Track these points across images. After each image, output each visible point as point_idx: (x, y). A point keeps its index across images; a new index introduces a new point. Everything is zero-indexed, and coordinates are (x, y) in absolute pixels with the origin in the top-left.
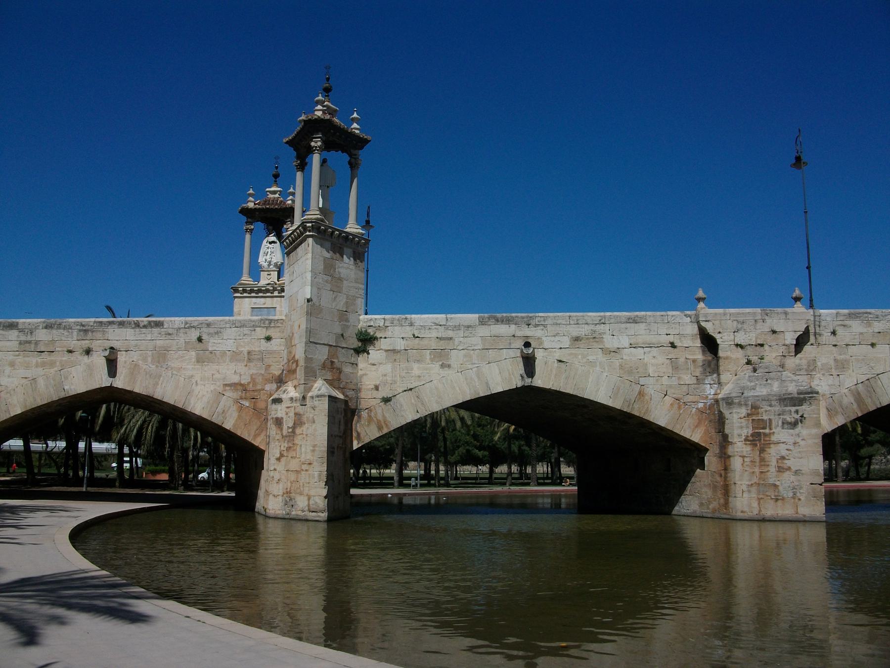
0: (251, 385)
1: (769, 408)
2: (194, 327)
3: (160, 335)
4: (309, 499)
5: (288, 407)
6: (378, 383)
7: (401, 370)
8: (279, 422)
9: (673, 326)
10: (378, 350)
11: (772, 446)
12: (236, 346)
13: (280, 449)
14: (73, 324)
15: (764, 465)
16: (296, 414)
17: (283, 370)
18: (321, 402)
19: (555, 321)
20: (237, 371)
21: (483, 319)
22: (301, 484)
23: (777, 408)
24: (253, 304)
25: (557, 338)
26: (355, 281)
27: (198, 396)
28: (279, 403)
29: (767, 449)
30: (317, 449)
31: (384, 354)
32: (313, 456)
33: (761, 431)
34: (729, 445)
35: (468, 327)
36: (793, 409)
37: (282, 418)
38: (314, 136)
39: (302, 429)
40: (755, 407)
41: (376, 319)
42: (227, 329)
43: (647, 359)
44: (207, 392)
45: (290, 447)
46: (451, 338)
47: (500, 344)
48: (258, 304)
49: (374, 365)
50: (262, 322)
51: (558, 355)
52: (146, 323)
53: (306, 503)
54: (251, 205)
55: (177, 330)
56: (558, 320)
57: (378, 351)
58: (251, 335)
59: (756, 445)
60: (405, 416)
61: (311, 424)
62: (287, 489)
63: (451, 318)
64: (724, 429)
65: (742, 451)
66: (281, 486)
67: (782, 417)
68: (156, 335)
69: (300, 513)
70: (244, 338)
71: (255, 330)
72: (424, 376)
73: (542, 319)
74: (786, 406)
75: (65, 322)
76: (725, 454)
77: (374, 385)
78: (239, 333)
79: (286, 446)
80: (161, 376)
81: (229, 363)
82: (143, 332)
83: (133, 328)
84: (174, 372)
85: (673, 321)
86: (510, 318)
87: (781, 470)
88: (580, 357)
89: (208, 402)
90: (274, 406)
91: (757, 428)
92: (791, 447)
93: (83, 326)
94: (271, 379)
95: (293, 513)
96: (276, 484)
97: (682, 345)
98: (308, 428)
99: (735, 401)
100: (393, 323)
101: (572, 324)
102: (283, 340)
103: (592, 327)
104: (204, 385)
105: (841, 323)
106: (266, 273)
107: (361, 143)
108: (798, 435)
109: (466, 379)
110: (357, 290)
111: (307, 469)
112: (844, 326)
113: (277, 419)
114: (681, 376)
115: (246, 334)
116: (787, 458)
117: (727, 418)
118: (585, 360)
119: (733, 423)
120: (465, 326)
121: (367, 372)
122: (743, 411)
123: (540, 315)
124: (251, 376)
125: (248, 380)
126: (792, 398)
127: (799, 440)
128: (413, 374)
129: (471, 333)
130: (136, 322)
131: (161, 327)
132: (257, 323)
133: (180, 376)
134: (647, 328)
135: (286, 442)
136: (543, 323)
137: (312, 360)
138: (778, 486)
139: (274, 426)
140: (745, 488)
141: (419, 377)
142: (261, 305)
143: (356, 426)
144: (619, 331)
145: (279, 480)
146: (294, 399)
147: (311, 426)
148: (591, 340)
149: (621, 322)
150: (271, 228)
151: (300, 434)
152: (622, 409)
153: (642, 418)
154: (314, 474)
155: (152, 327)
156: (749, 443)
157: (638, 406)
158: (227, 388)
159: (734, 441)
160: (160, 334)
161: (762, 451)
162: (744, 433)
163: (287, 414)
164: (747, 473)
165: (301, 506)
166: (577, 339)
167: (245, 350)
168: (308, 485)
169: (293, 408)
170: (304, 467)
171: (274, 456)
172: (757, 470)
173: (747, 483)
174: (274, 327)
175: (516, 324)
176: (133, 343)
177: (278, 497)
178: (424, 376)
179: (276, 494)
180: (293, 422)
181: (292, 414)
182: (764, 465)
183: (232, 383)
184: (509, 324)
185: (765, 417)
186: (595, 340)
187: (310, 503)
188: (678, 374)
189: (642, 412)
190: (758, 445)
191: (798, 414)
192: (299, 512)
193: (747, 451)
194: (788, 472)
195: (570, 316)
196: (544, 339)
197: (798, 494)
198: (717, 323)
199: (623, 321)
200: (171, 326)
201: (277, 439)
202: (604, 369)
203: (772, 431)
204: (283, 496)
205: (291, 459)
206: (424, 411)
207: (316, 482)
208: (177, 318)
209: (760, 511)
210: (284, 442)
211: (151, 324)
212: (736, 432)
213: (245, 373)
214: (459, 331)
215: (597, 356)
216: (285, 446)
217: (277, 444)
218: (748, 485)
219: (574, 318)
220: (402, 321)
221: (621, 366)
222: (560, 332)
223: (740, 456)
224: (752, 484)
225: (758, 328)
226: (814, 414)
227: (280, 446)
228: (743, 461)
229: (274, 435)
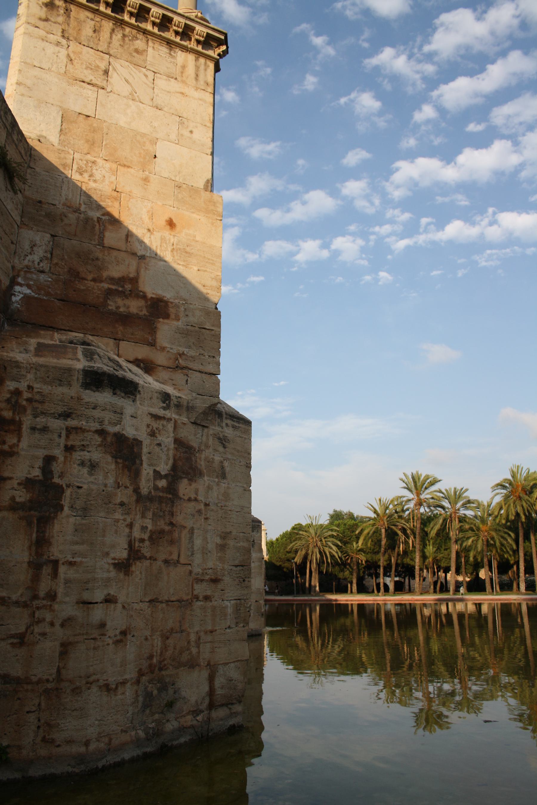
13: (130, 535)
16: (178, 442)
18: (238, 433)
22: (193, 637)
28: (126, 393)
30: (231, 543)
32: (221, 559)
39: (194, 485)
45: (162, 532)
61: (217, 480)
62: (151, 657)
79: (150, 527)
96: (112, 647)
111: (209, 593)
135: (150, 514)
145: (124, 633)
146: (174, 401)
147: (218, 484)
151: (190, 500)
163: (152, 434)
165: (193, 699)
168: (209, 638)
170: (200, 589)
177: (120, 690)
179: (112, 680)
180: (171, 462)
201: (118, 501)
204: (138, 682)
210: (143, 516)
216: (144, 528)
217: (117, 516)
227: (131, 526)
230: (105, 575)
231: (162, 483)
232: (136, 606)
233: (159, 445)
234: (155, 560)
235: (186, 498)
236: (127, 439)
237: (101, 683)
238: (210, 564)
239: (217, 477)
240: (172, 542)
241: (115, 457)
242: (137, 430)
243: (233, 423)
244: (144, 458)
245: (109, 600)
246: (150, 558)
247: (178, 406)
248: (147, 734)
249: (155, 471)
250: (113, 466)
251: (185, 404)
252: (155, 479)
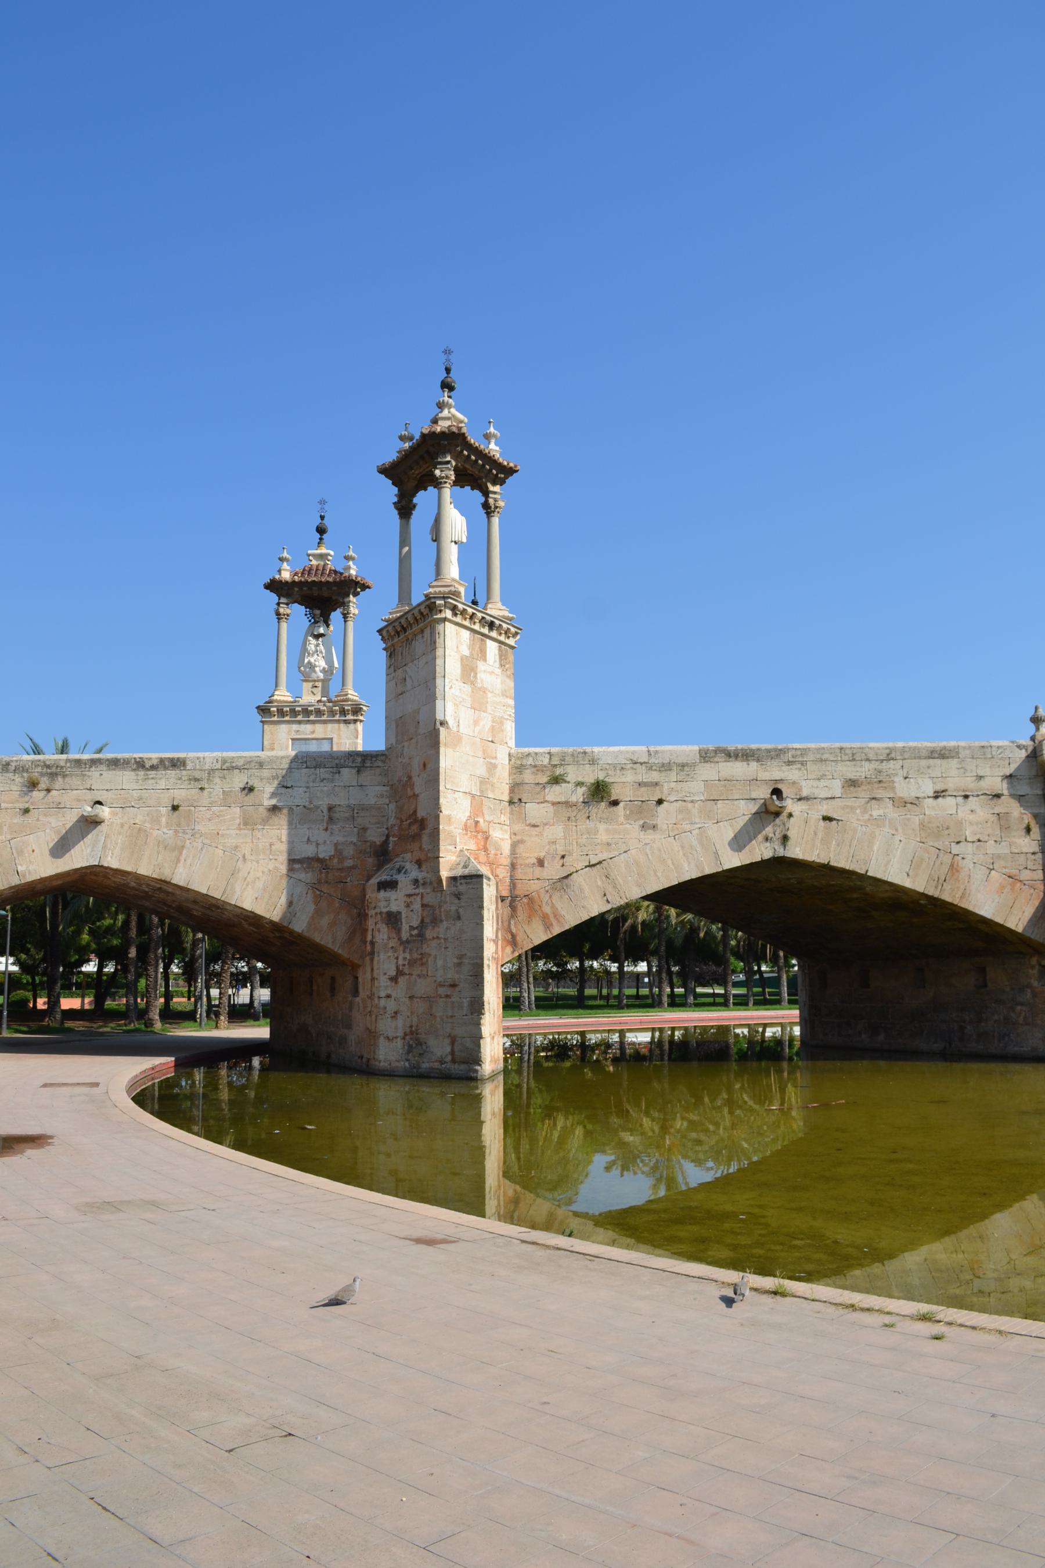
0: (336, 860)
2: (236, 768)
3: (179, 782)
4: (453, 1043)
5: (409, 896)
6: (542, 854)
7: (579, 833)
8: (393, 919)
9: (1000, 762)
10: (542, 803)
12: (308, 798)
13: (397, 963)
14: (30, 764)
16: (423, 905)
17: (388, 836)
18: (471, 887)
19: (818, 756)
20: (310, 838)
21: (706, 754)
24: (293, 733)
25: (823, 783)
26: (502, 692)
27: (248, 879)
30: (466, 961)
31: (551, 809)
32: (457, 972)
35: (683, 766)
37: (399, 913)
38: (439, 460)
39: (436, 929)
41: (536, 754)
42: (293, 770)
43: (963, 813)
44: (263, 872)
46: (657, 784)
47: (734, 791)
48: (304, 733)
49: (534, 826)
50: (351, 759)
51: (825, 809)
52: (155, 762)
53: (448, 1049)
54: (286, 576)
55: (209, 774)
56: (822, 754)
57: (542, 805)
58: (333, 780)
60: (588, 906)
62: (411, 1027)
63: (657, 752)
66: (400, 1022)
68: (173, 780)
69: (436, 1065)
70: (322, 784)
71: (339, 772)
72: (616, 844)
73: (799, 753)
75: (17, 761)
77: (537, 858)
78: (314, 776)
79: (408, 957)
80: (183, 847)
81: (298, 826)
82: (150, 776)
83: (134, 770)
84: (207, 841)
85: (1000, 756)
86: (748, 751)
88: (858, 811)
89: (264, 890)
90: (382, 894)
93: (48, 767)
94: (368, 850)
95: (425, 1066)
96: (390, 1020)
98: (447, 928)
100: (564, 760)
101: (845, 761)
102: (388, 788)
103: (875, 765)
104: (258, 862)
106: (311, 684)
107: (504, 473)
109: (682, 847)
110: (505, 708)
111: (449, 993)
113: (390, 914)
114: (1014, 840)
115: (324, 779)
118: (867, 817)
120: (678, 765)
121: (524, 838)
123: (795, 747)
124: (336, 845)
125: (330, 852)
128: (599, 841)
129: (688, 775)
130: (138, 760)
131: (182, 768)
132: (342, 761)
133: (217, 847)
134: (960, 766)
135: (408, 951)
136: (800, 759)
137: (450, 820)
139: (384, 926)
141: (608, 844)
142: (306, 734)
143: (510, 923)
144: (918, 771)
145: (396, 1013)
146: (421, 882)
147: (454, 924)
148: (876, 785)
149: (920, 758)
150: (318, 612)
151: (434, 938)
152: (926, 892)
153: (956, 906)
154: (463, 1002)
155: (166, 768)
157: (950, 887)
158: (297, 866)
160: (180, 779)
163: (408, 906)
165: (439, 1054)
166: (852, 783)
167: (323, 803)
168: (450, 1020)
169: (420, 896)
170: (442, 991)
171: (385, 974)
174: (371, 767)
175: (758, 760)
176: (136, 794)
177: (395, 1041)
178: (616, 844)
179: (390, 1035)
181: (417, 906)
183: (304, 858)
184: (747, 760)
186: (880, 785)
187: (456, 1049)
188: (1009, 837)
189: (957, 896)
192: (436, 1064)
195: (841, 749)
196: (803, 783)
199: (923, 755)
200: (198, 767)
202: (897, 830)
204: (404, 1038)
205: (417, 978)
206: (618, 899)
207: (466, 1015)
208: (207, 754)
210: (404, 952)
211: (165, 764)
213: (325, 842)
214: (669, 772)
215: (886, 811)
216: (405, 959)
217: (390, 954)
219: (848, 751)
220: (577, 757)
221: (922, 825)
222: (827, 773)
227: (397, 958)
229: (385, 941)
230: (385, 984)
231: (415, 932)
232: (401, 1000)
233: (412, 911)
234: (412, 975)
235: (431, 937)
236: (393, 913)
237: (385, 1035)
238: (449, 976)
239: (454, 920)
240: (422, 964)
241: (387, 924)
242: (398, 906)
243: (466, 881)
244: (403, 921)
245: (388, 996)
246: (409, 974)
247: (424, 884)
248: (410, 1065)
249: (410, 926)
250: (386, 930)
251: (429, 881)
252: (410, 930)
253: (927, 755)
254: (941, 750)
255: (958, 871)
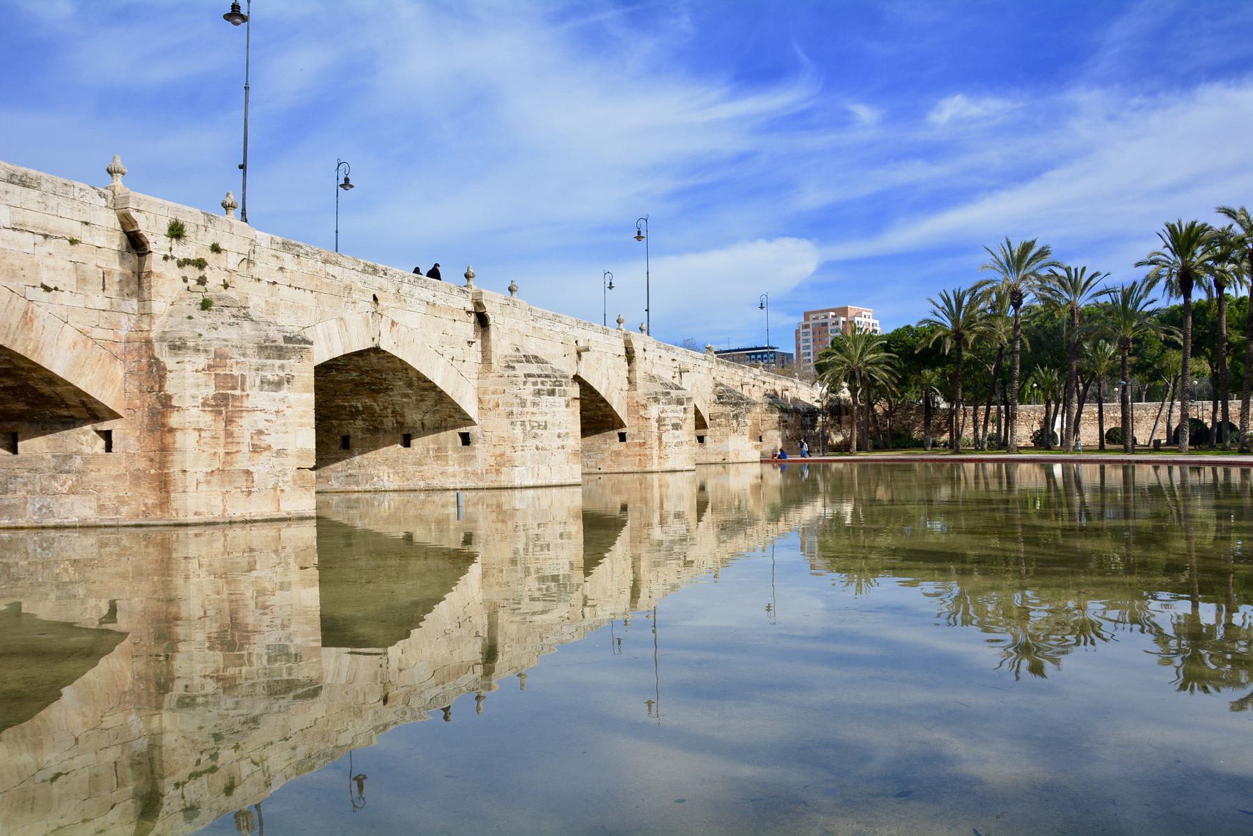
1: (242, 359)
11: (244, 414)
15: (232, 443)
23: (255, 361)
29: (237, 420)
33: (229, 392)
34: (171, 412)
36: (278, 362)
40: (221, 357)
59: (220, 413)
64: (161, 388)
65: (198, 422)
67: (260, 373)
74: (268, 357)
76: (163, 425)
85: (82, 200)
87: (256, 449)
91: (223, 388)
92: (273, 417)
97: (91, 242)
99: (188, 344)
105: (274, 252)
108: (283, 400)
112: (278, 257)
116: (266, 432)
117: (168, 369)
119: (184, 377)
122: (202, 361)
126: (276, 347)
127: (282, 407)
134: (41, 201)
138: (252, 473)
140: (202, 479)
156: (210, 409)
159: (184, 407)
161: (229, 421)
162: (202, 394)
164: (205, 454)
172: (221, 451)
173: (205, 470)
182: (232, 443)
185: (236, 372)
189: (29, 348)
190: (224, 412)
191: (283, 371)
193: (206, 422)
194: (266, 453)
197: (281, 484)
198: (151, 217)
203: (245, 393)
209: (225, 510)
212: (189, 392)
218: (207, 473)
223: (194, 429)
224: (212, 472)
225: (199, 237)
226: (305, 372)
228: (200, 436)
253: (5, 177)
254: (22, 176)
255: (31, 320)
